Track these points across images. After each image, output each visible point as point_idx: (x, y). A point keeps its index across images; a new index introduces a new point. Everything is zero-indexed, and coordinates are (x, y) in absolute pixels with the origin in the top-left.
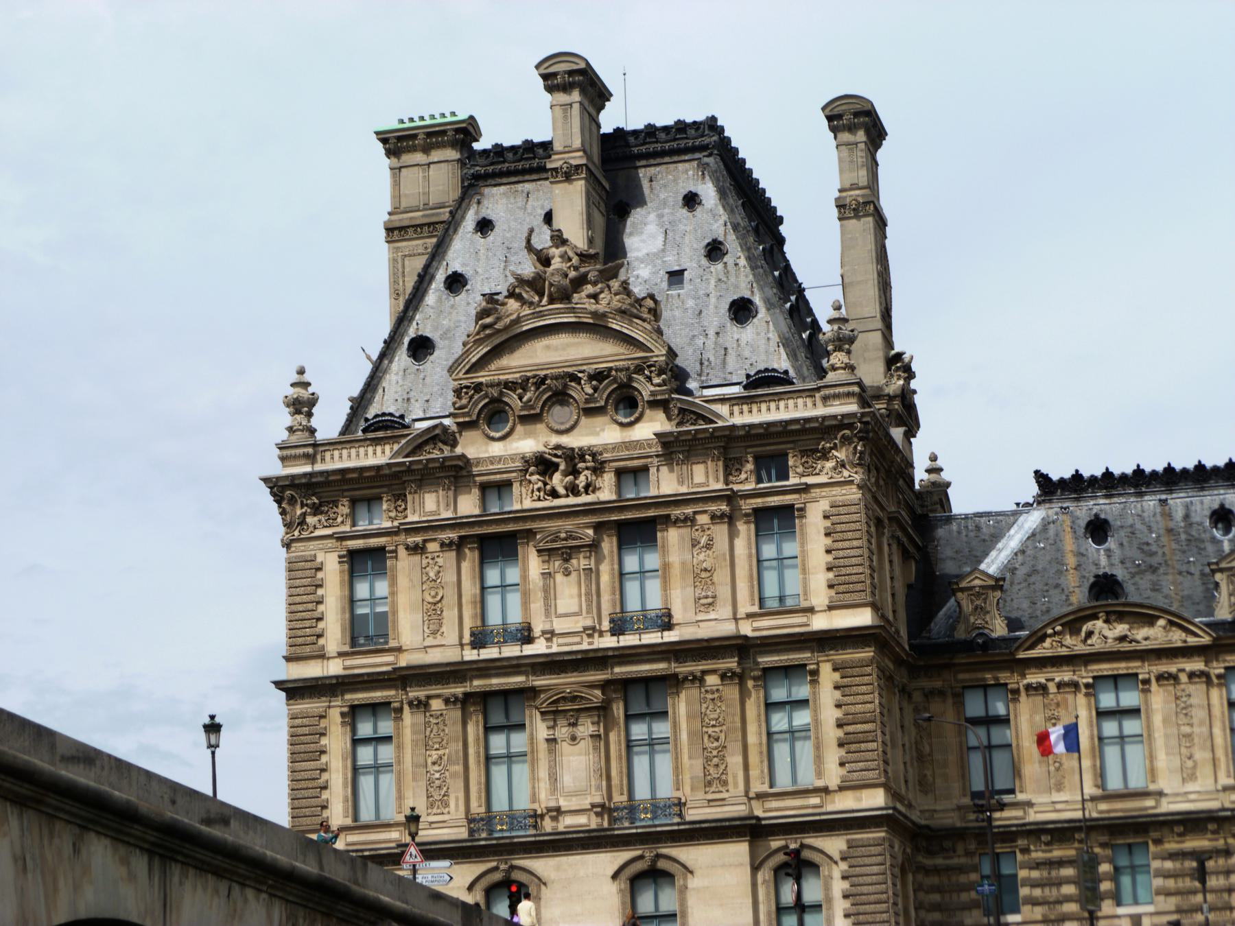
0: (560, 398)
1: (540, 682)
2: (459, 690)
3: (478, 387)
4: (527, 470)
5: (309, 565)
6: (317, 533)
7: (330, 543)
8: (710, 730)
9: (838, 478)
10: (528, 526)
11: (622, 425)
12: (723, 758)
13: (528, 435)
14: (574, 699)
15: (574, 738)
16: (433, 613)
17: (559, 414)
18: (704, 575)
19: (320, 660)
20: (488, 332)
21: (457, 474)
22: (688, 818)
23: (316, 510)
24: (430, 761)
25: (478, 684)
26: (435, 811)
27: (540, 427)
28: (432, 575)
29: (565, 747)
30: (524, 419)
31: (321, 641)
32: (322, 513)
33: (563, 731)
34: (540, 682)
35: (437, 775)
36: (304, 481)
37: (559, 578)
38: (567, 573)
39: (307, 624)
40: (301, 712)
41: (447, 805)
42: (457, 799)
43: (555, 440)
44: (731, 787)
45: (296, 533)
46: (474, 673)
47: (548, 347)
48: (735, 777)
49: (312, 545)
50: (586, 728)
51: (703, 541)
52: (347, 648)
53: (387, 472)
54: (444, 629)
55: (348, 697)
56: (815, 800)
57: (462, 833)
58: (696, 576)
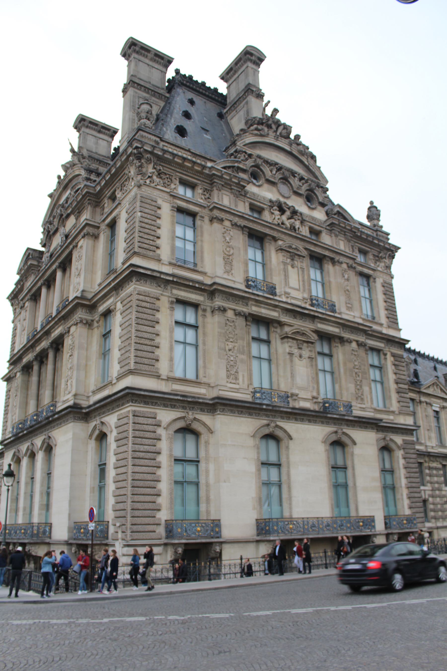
0: (285, 180)
1: (284, 319)
2: (245, 310)
3: (250, 156)
4: (272, 207)
5: (154, 204)
6: (158, 187)
7: (167, 197)
8: (356, 370)
9: (385, 271)
10: (275, 234)
11: (309, 207)
12: (361, 386)
13: (270, 191)
14: (303, 334)
15: (301, 356)
16: (228, 261)
17: (284, 189)
18: (347, 292)
19: (157, 263)
20: (256, 132)
21: (240, 191)
22: (353, 415)
23: (159, 174)
24: (227, 348)
25: (255, 309)
26: (230, 380)
27: (274, 189)
28: (228, 239)
29: (296, 360)
30: (268, 181)
31: (158, 252)
32: (161, 178)
33: (296, 351)
34: (284, 319)
35: (232, 358)
36: (160, 153)
37: (290, 267)
38: (293, 267)
39: (152, 238)
40: (145, 292)
41: (236, 379)
42: (243, 376)
43: (282, 200)
44: (366, 402)
45: (148, 182)
46: (253, 303)
47: (277, 156)
48: (367, 397)
49: (156, 193)
50: (306, 353)
51: (346, 276)
52: (174, 262)
53: (207, 171)
54: (233, 272)
55: (175, 292)
56: (391, 417)
57: (248, 398)
58: (345, 291)
